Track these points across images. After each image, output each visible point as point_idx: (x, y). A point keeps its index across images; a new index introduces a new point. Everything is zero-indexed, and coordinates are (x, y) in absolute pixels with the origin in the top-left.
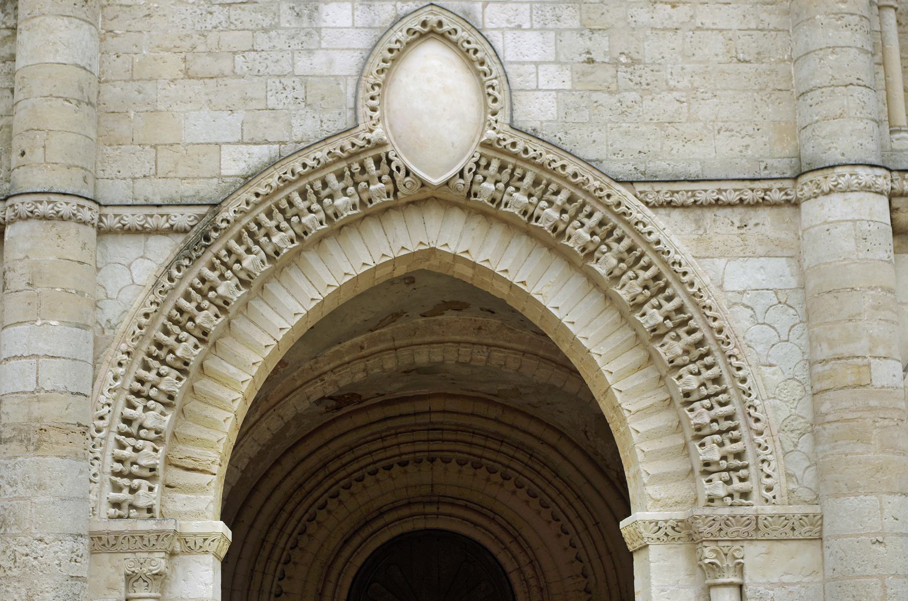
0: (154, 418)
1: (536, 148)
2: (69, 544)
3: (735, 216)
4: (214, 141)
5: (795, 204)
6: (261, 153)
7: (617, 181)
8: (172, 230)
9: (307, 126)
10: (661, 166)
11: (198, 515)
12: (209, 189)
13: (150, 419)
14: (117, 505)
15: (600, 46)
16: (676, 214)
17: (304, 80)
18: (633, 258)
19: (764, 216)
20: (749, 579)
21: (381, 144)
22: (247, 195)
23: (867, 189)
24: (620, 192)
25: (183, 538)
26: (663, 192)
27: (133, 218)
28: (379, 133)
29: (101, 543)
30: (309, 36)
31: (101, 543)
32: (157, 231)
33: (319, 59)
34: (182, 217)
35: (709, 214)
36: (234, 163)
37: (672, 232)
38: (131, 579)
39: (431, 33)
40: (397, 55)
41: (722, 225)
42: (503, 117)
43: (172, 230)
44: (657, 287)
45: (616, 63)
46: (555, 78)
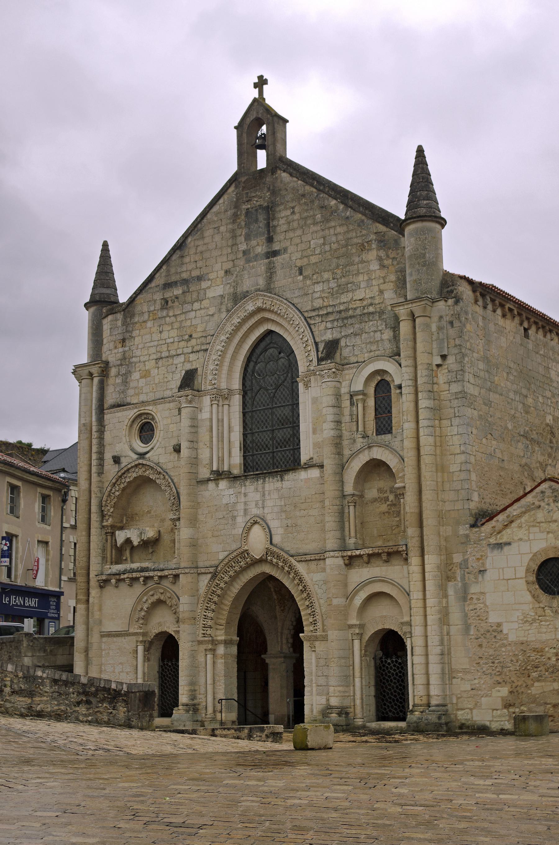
0: (210, 614)
1: (275, 549)
2: (191, 643)
3: (315, 562)
4: (217, 551)
5: (325, 559)
6: (226, 553)
7: (292, 556)
8: (210, 573)
9: (234, 547)
10: (301, 551)
11: (221, 635)
12: (217, 562)
13: (209, 615)
14: (204, 634)
15: (289, 522)
16: (304, 563)
17: (234, 535)
18: (296, 573)
19: (321, 562)
20: (317, 649)
21: (247, 550)
22: (222, 564)
23: (333, 557)
24: (291, 558)
25: (217, 640)
26: (299, 558)
27: (203, 570)
28: (246, 548)
29: (200, 643)
30: (234, 525)
31: (200, 643)
32: (207, 573)
33: (236, 530)
34: (212, 570)
35: (310, 562)
36: (221, 556)
37: (301, 568)
38: (206, 650)
39: (256, 523)
40: (249, 529)
41: (313, 565)
42: (269, 542)
43: (210, 573)
44: (301, 580)
45: (292, 526)
46: (281, 531)
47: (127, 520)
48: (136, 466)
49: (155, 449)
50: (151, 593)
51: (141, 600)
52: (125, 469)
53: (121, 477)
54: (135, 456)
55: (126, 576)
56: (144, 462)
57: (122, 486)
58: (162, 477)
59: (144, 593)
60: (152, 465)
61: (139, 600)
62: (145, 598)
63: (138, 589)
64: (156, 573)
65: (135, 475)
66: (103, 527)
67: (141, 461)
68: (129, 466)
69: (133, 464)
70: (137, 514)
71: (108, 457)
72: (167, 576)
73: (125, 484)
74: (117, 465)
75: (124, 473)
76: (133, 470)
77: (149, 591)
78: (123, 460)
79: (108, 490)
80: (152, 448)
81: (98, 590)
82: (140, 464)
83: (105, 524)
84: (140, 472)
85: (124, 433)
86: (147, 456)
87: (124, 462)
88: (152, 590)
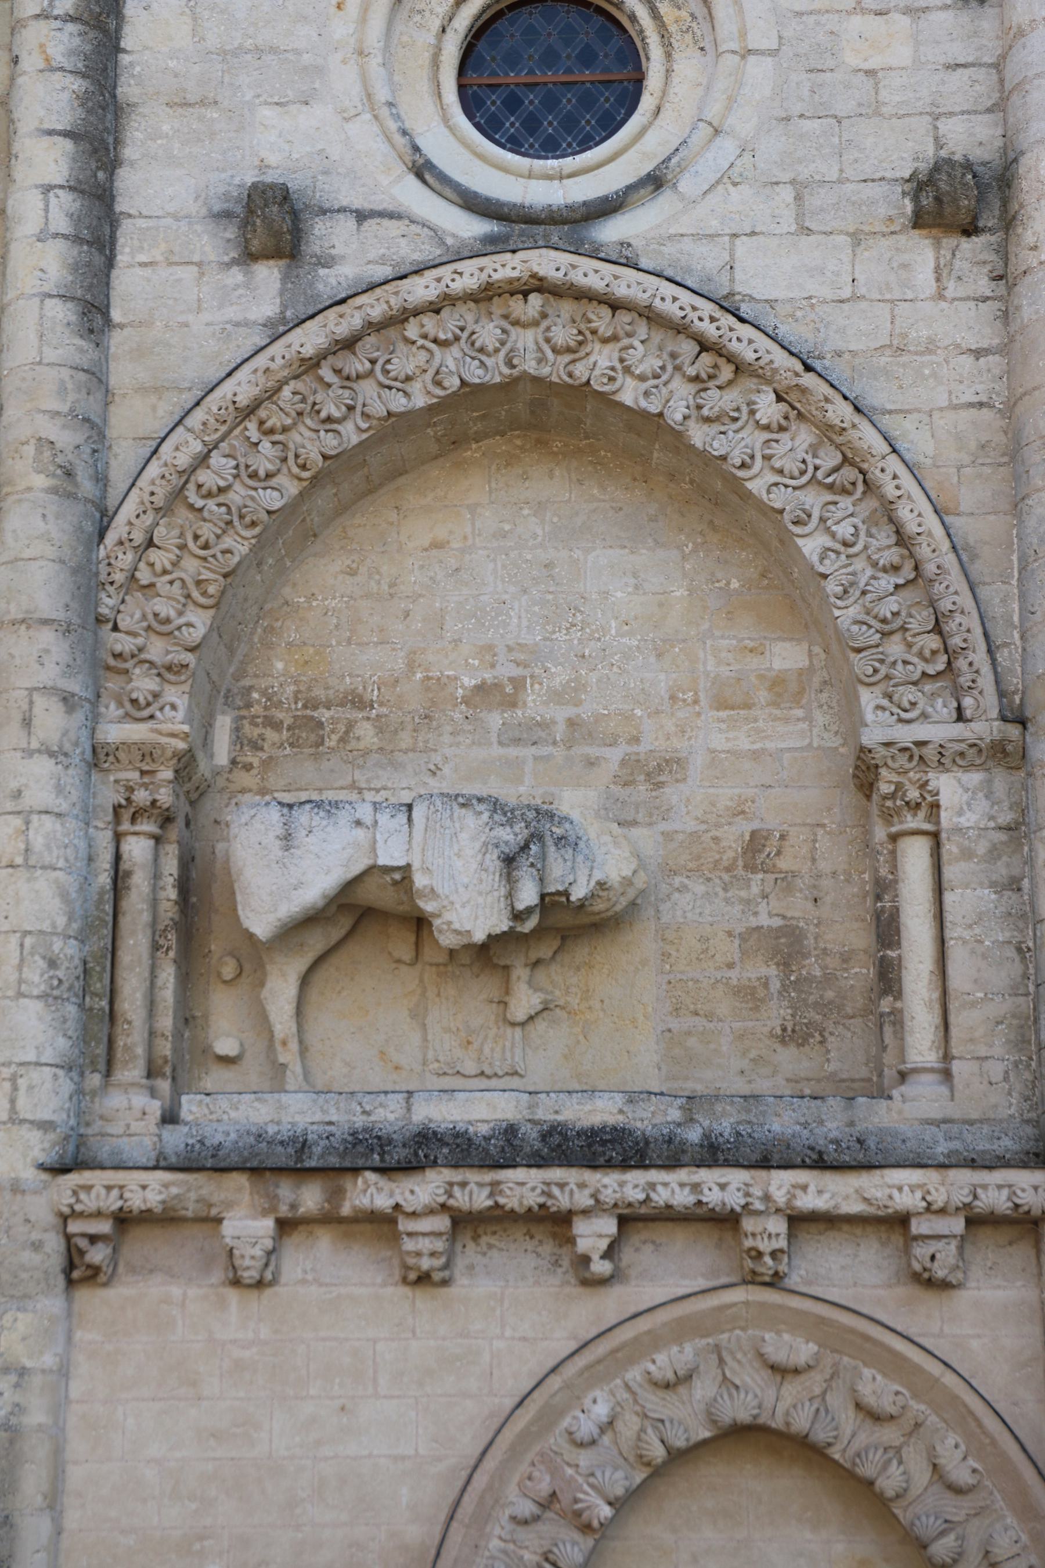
47: (238, 738)
48: (486, 295)
49: (686, 184)
50: (664, 1362)
51: (549, 1417)
52: (374, 306)
53: (310, 365)
54: (471, 228)
55: (424, 1190)
56: (590, 274)
57: (312, 444)
58: (768, 408)
59: (595, 1358)
60: (672, 301)
61: (533, 1412)
62: (601, 1410)
63: (511, 1319)
64: (780, 1183)
65: (457, 367)
66: (99, 757)
67: (548, 263)
68: (421, 290)
69: (469, 276)
70: (358, 701)
71: (168, 185)
72: (901, 1221)
73: (351, 434)
74: (268, 275)
75: (349, 344)
76: (448, 324)
77: (654, 1341)
78: (331, 235)
79: (184, 448)
80: (655, 182)
81: (53, 1304)
82: (538, 285)
83: (116, 731)
84: (530, 347)
85: (342, 28)
86: (610, 232)
87: (349, 254)
88: (683, 1330)
